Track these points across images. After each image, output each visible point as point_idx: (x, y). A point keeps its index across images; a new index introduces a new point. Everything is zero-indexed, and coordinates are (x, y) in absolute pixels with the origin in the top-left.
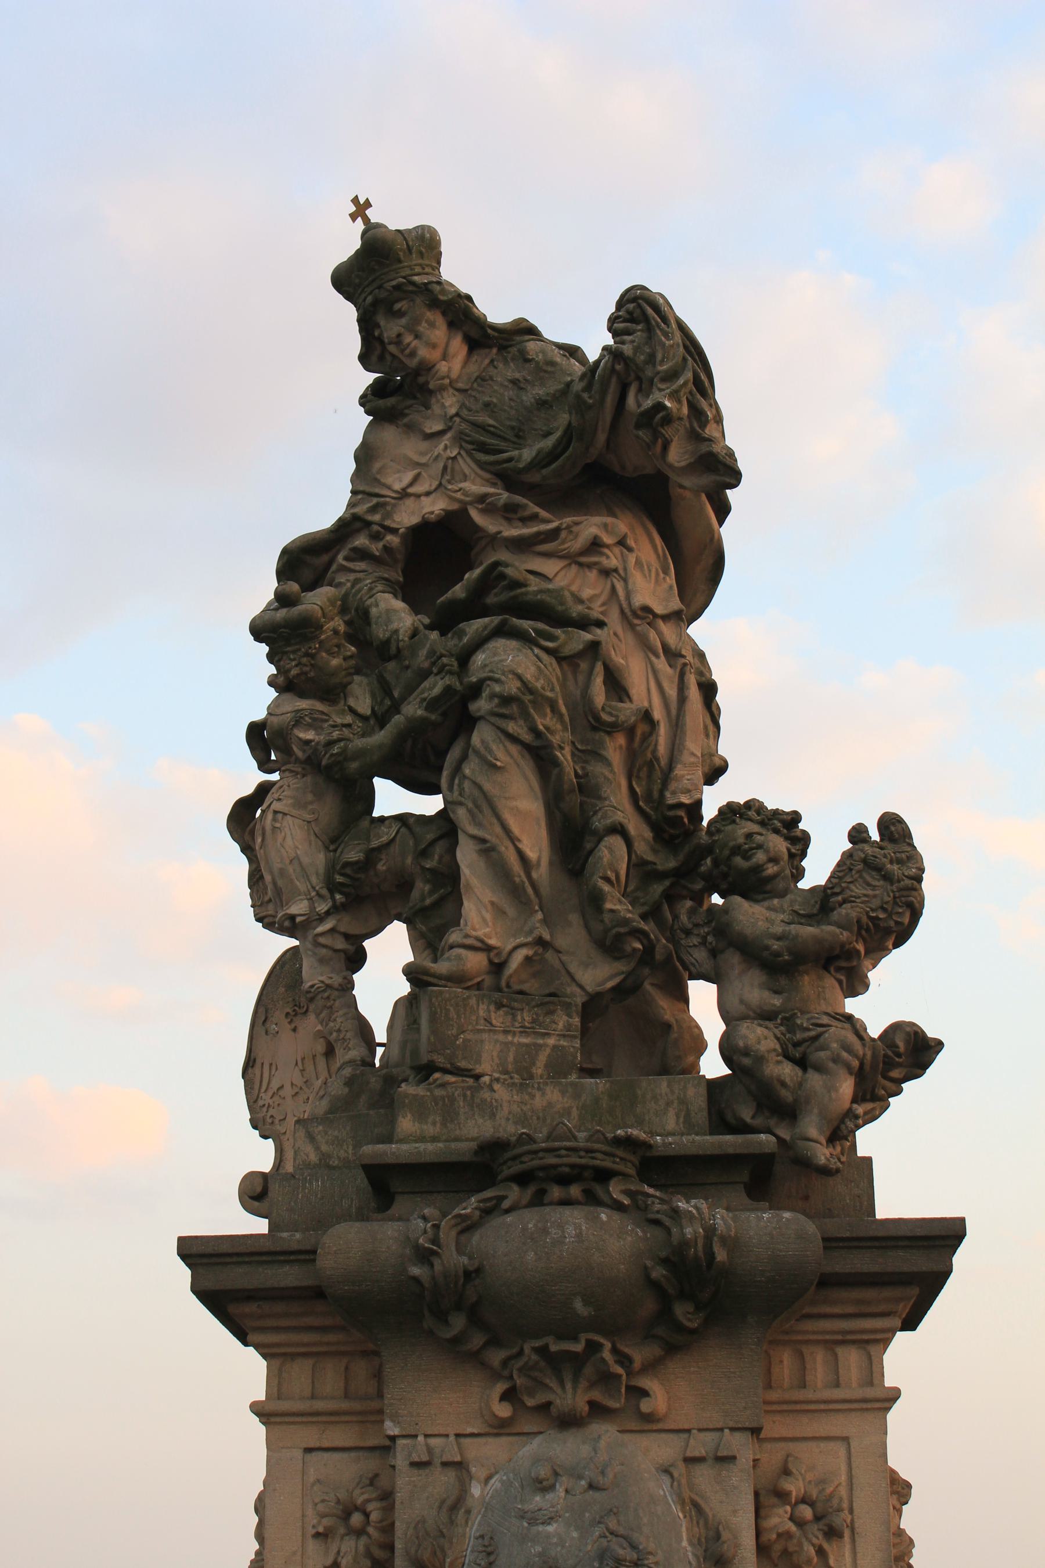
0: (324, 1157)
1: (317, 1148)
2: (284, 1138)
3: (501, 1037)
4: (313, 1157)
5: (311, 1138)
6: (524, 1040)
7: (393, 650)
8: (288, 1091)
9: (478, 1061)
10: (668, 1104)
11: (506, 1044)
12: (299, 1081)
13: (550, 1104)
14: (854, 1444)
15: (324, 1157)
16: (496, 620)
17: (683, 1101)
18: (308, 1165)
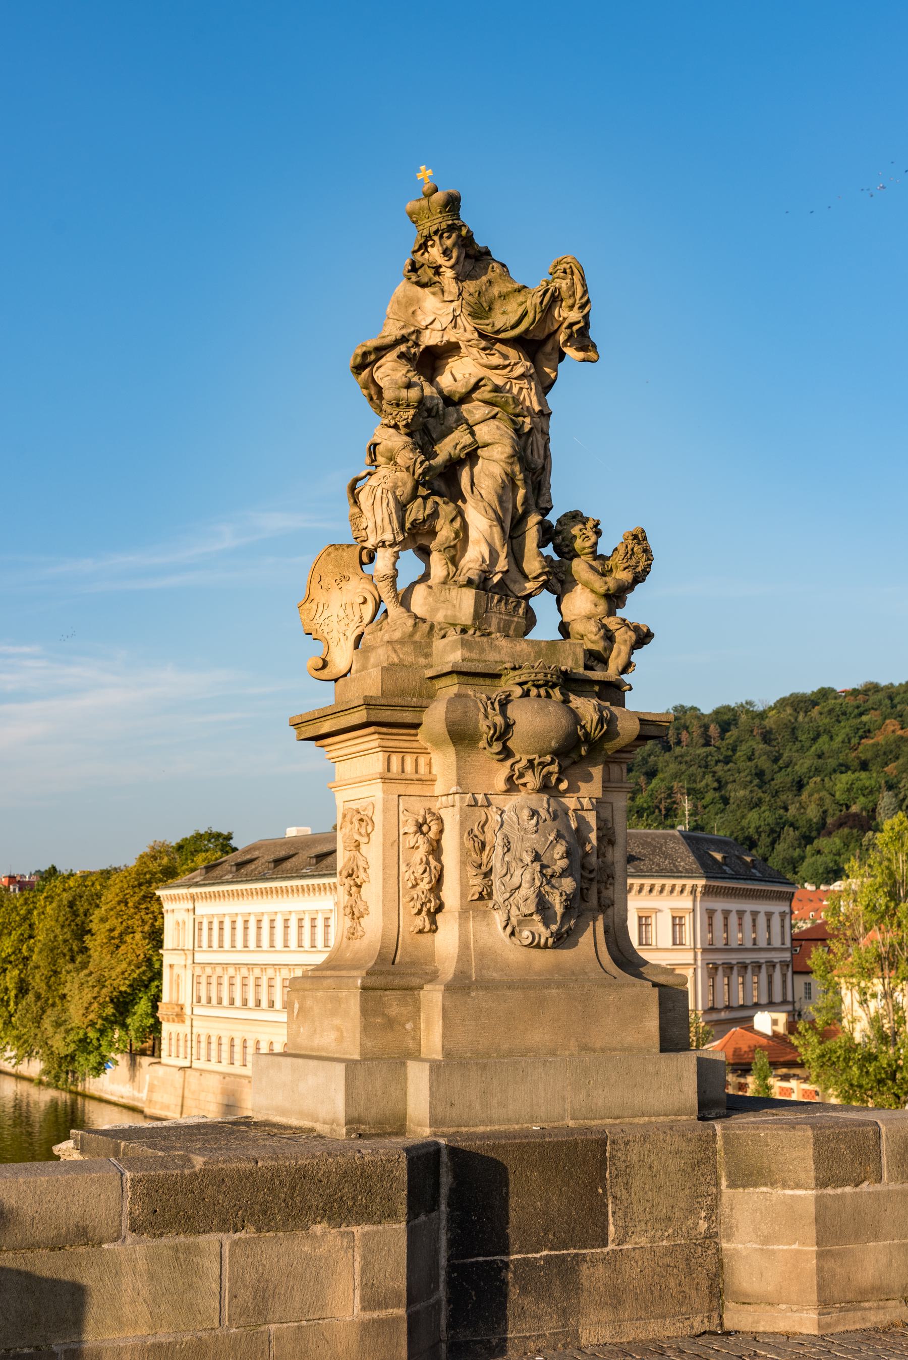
0: (401, 660)
1: (398, 656)
2: (330, 642)
3: (498, 615)
4: (396, 660)
5: (395, 651)
6: (507, 618)
7: (434, 413)
8: (334, 618)
9: (490, 626)
10: (569, 654)
11: (501, 619)
12: (342, 614)
13: (521, 651)
14: (614, 805)
15: (401, 660)
16: (497, 409)
17: (574, 653)
18: (393, 664)
